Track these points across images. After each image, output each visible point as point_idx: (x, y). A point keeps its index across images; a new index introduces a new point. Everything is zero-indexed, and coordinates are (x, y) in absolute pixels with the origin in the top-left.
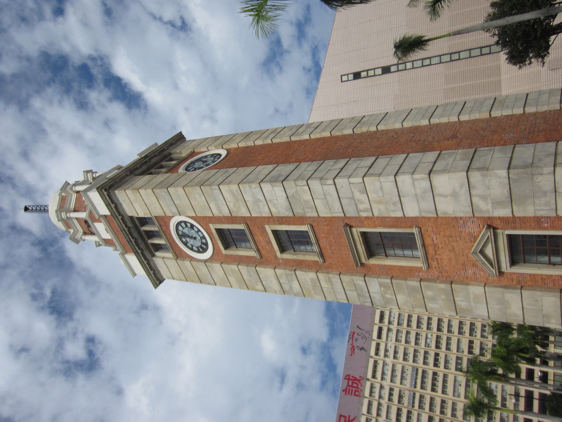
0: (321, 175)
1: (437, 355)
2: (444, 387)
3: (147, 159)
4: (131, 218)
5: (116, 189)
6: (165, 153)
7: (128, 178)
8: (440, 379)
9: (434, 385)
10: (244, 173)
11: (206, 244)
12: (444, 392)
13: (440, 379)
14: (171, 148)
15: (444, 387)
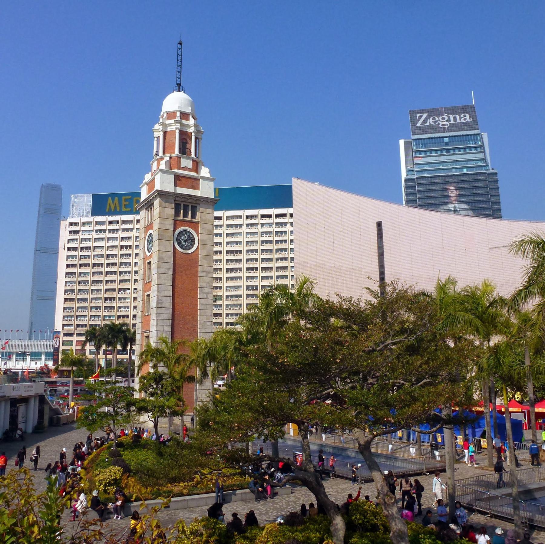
0: (160, 324)
1: (256, 269)
2: (232, 278)
3: (188, 197)
4: (153, 204)
5: (160, 197)
6: (199, 202)
7: (171, 197)
8: (237, 275)
9: (232, 270)
10: (166, 281)
11: (149, 252)
12: (227, 278)
13: (237, 275)
14: (204, 202)
15: (232, 278)
